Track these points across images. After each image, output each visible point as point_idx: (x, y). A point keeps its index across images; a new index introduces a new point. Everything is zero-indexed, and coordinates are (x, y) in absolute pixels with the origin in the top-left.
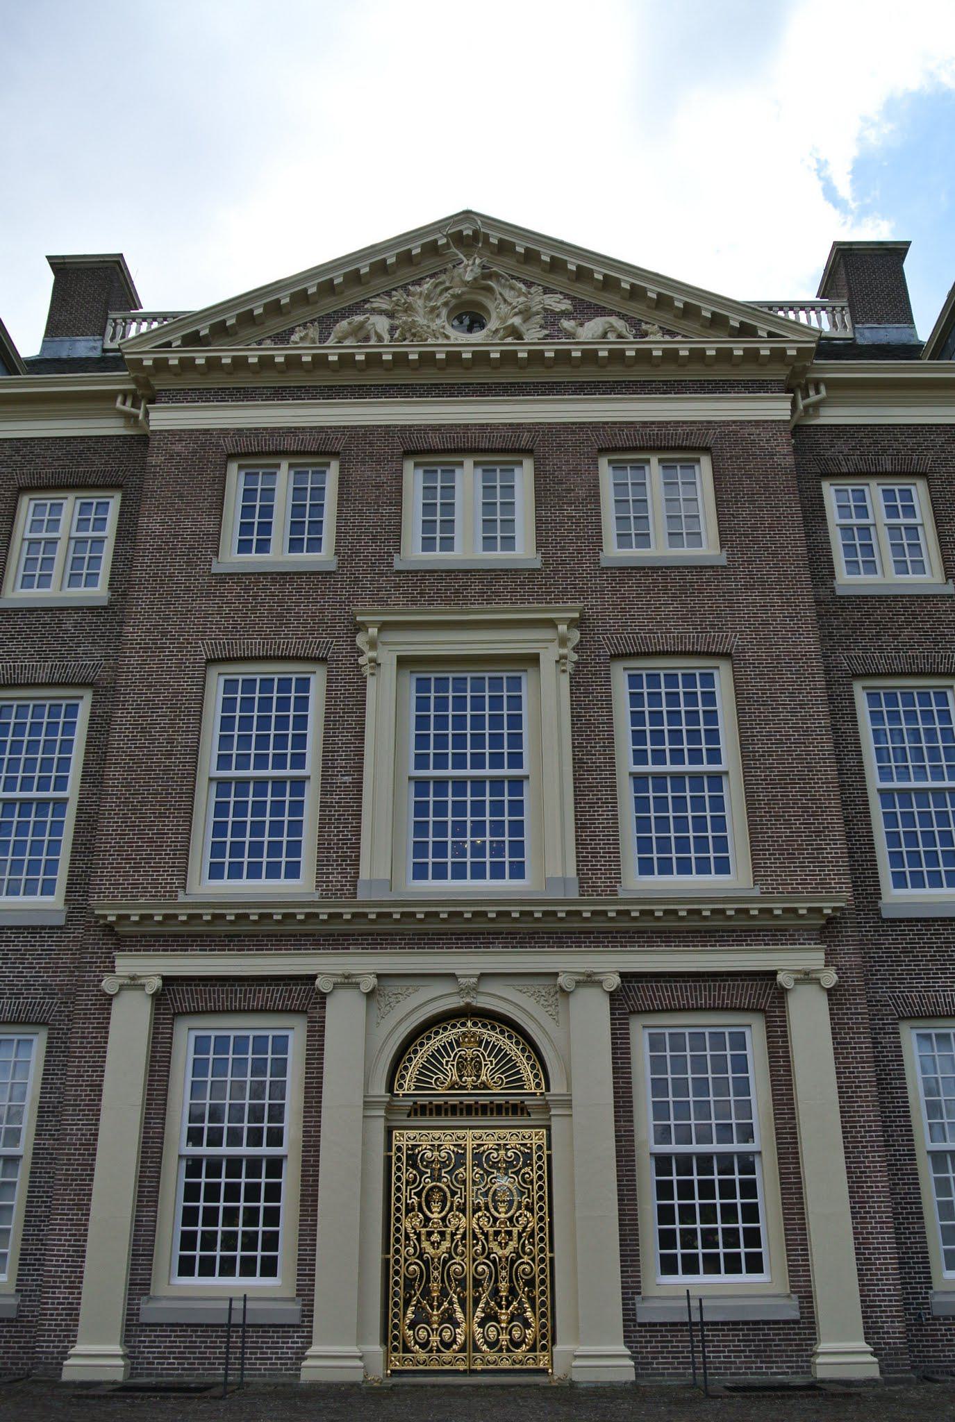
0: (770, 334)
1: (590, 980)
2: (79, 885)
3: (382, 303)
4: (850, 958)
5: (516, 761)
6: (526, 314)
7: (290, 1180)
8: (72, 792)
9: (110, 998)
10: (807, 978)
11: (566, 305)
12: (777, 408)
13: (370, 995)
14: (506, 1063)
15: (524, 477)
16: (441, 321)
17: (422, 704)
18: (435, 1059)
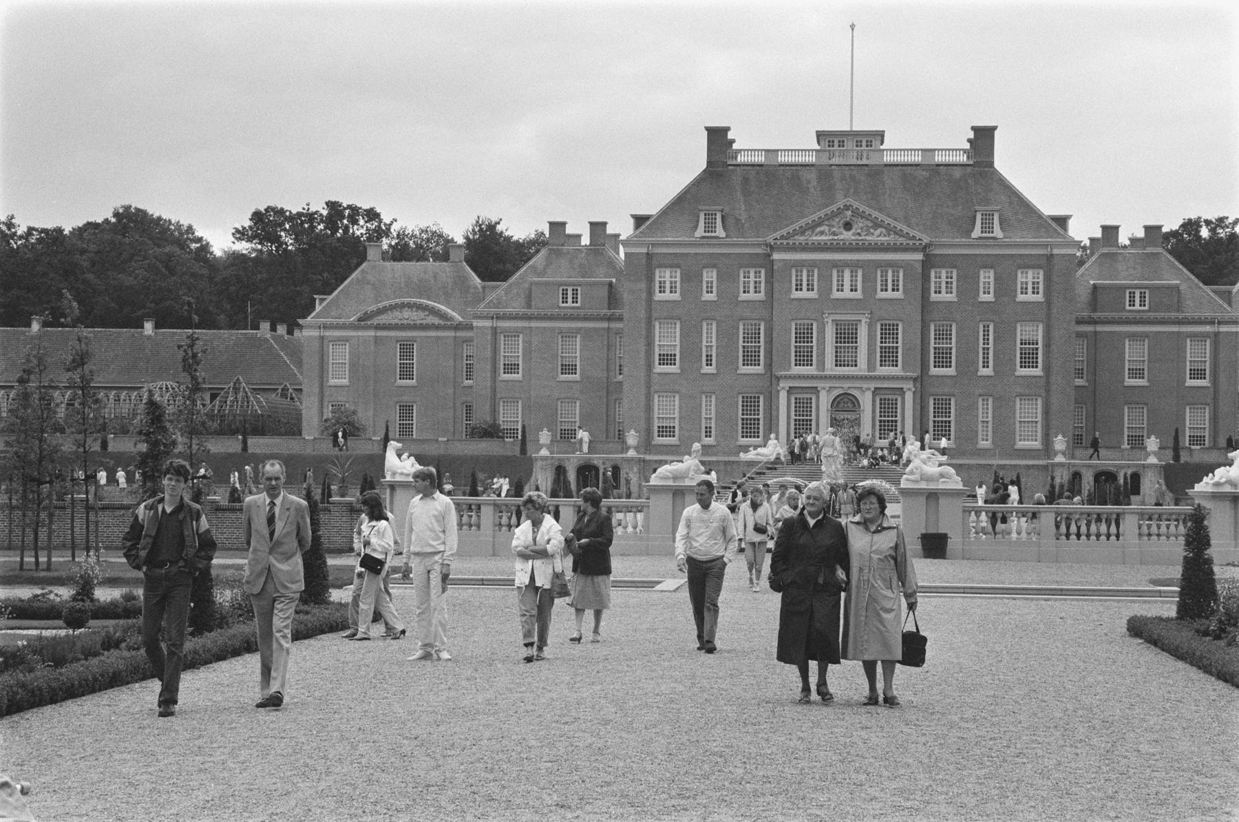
0: (920, 239)
1: (869, 389)
2: (769, 366)
3: (826, 223)
4: (918, 385)
5: (856, 342)
6: (862, 229)
7: (814, 423)
8: (762, 343)
9: (779, 391)
10: (909, 389)
11: (870, 225)
12: (919, 256)
13: (828, 391)
14: (853, 403)
15: (860, 273)
16: (842, 230)
17: (837, 329)
18: (839, 403)
